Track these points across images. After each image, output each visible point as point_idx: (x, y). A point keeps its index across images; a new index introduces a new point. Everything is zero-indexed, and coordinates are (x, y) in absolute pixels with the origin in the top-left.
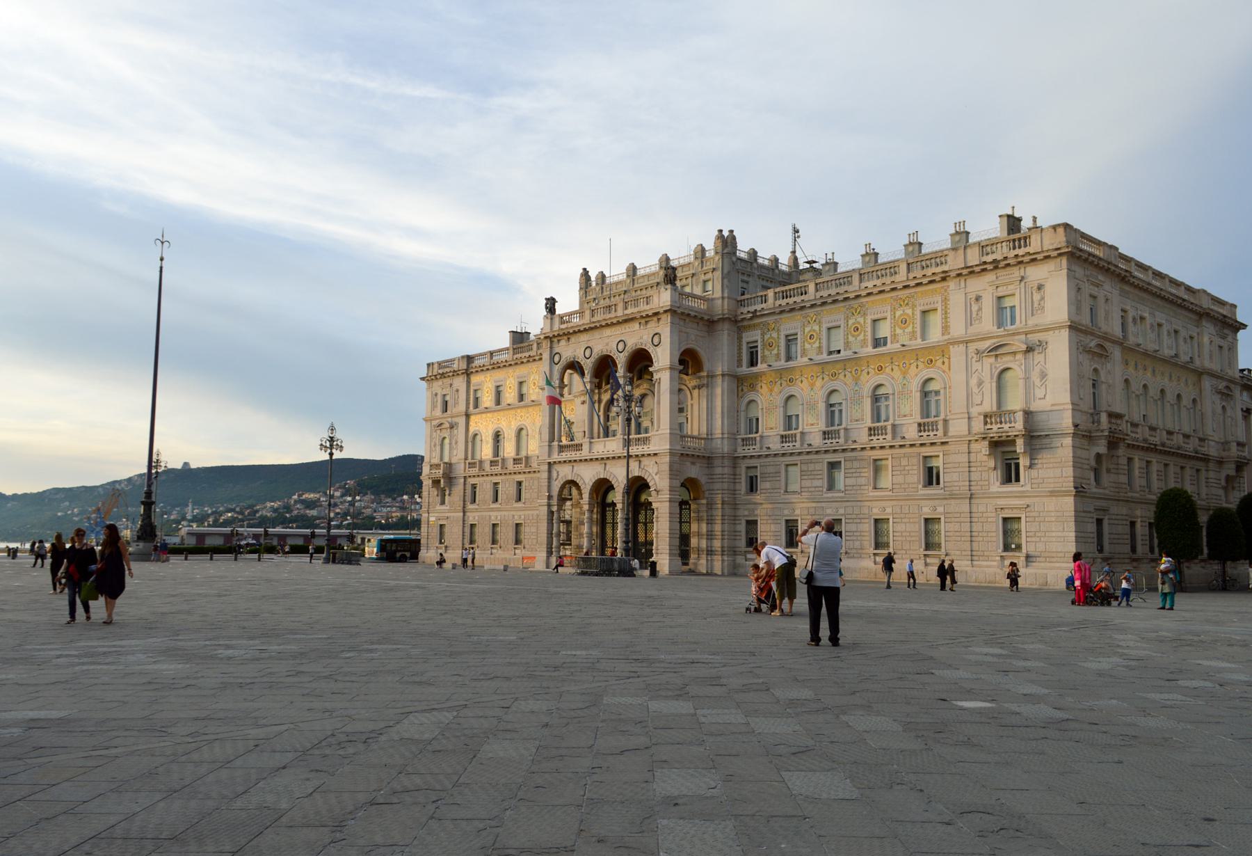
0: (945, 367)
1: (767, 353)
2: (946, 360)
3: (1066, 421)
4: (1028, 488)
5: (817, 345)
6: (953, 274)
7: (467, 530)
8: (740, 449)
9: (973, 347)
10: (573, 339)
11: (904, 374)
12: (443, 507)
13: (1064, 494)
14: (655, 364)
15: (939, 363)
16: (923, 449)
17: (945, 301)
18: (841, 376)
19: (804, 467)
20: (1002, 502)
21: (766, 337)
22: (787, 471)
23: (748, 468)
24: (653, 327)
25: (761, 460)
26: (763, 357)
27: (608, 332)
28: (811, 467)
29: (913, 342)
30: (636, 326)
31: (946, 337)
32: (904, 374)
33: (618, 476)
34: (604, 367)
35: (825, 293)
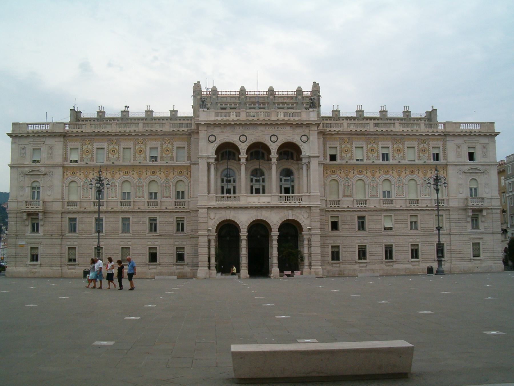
1: (343, 154)
2: (445, 172)
3: (496, 203)
4: (483, 230)
7: (66, 251)
8: (329, 206)
9: (459, 167)
10: (228, 128)
12: (35, 234)
13: (497, 233)
14: (303, 153)
18: (391, 173)
20: (472, 236)
21: (343, 146)
24: (304, 131)
27: (262, 128)
29: (429, 161)
30: (288, 128)
31: (445, 161)
33: (275, 220)
34: (258, 151)
35: (379, 129)
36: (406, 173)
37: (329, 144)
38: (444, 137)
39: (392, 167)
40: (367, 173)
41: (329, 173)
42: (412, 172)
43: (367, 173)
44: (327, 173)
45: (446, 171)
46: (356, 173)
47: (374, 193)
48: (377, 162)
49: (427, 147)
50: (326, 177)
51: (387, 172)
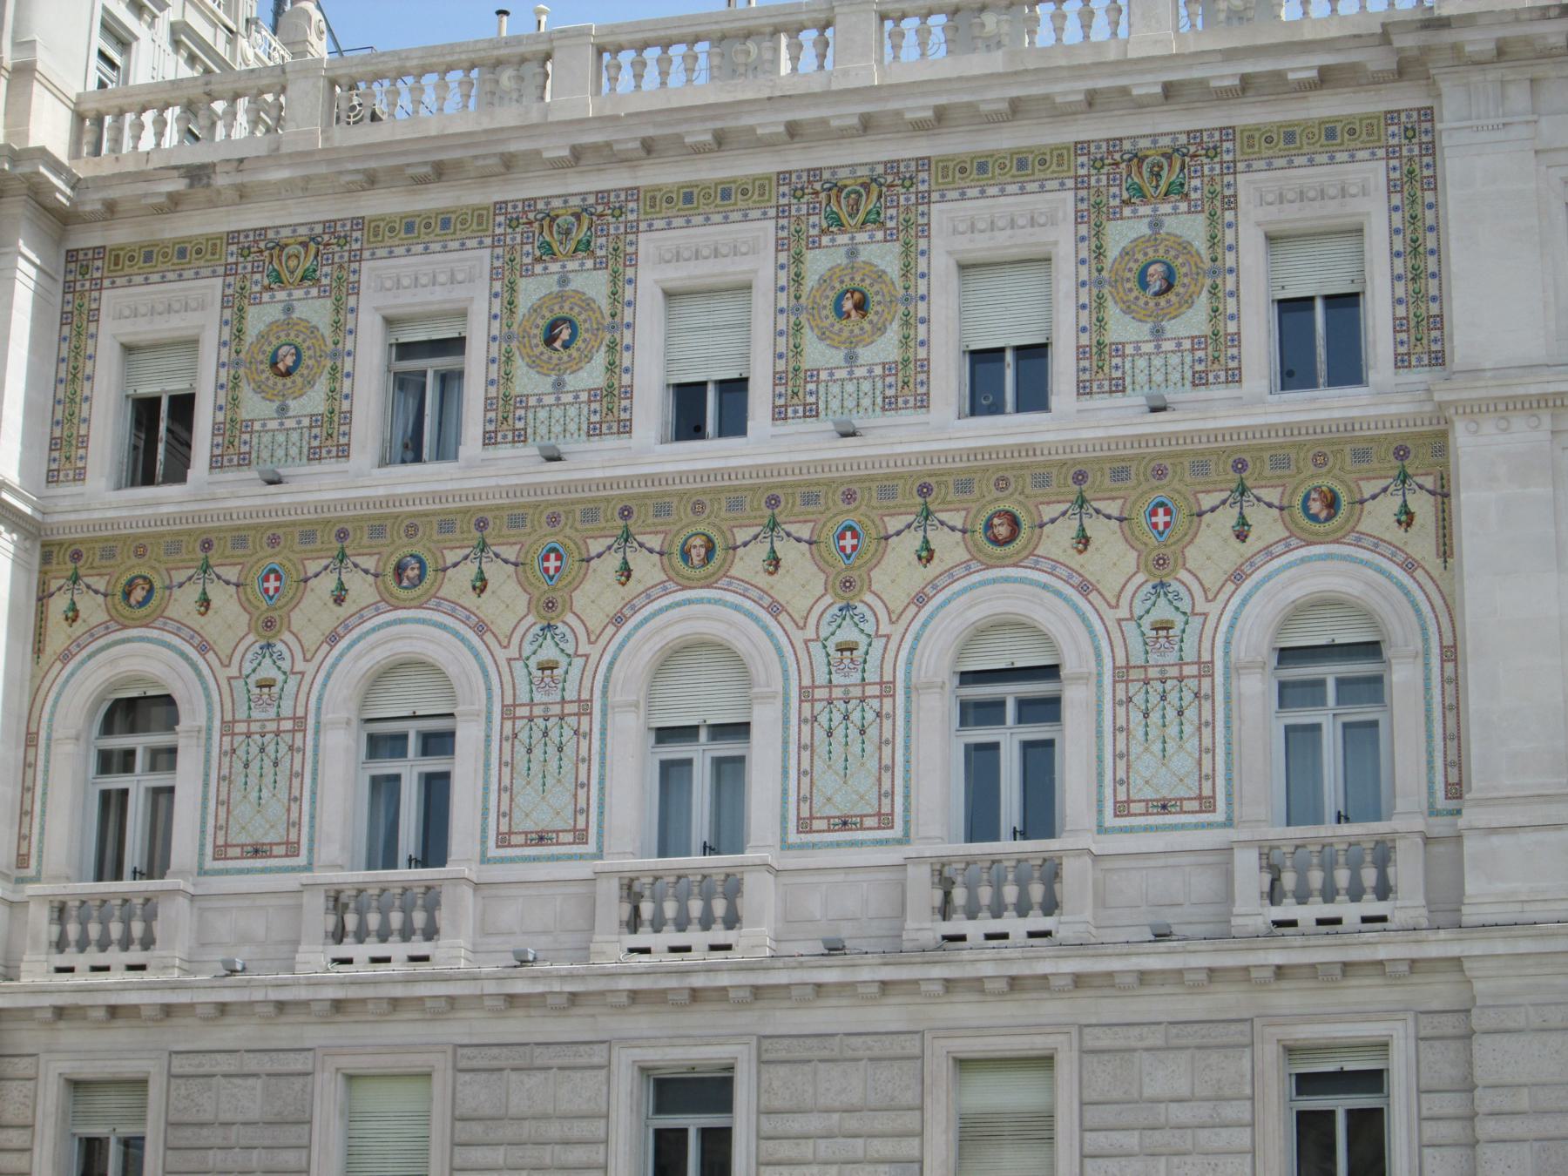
0: (1421, 543)
1: (254, 406)
2: (1423, 506)
5: (592, 375)
6: (1478, 42)
11: (1160, 566)
15: (1380, 516)
16: (1287, 999)
17: (1416, 184)
19: (478, 1095)
22: (351, 1116)
23: (77, 1086)
25: (182, 1036)
26: (230, 430)
28: (525, 1093)
32: (1160, 566)
36: (926, 554)
37: (122, 313)
38: (1406, 98)
39: (773, 503)
40: (480, 585)
41: (93, 609)
42: (1005, 532)
43: (480, 585)
44: (73, 615)
45: (1443, 494)
46: (361, 588)
47: (542, 808)
48: (597, 462)
49: (1189, 227)
50: (65, 657)
51: (701, 558)
